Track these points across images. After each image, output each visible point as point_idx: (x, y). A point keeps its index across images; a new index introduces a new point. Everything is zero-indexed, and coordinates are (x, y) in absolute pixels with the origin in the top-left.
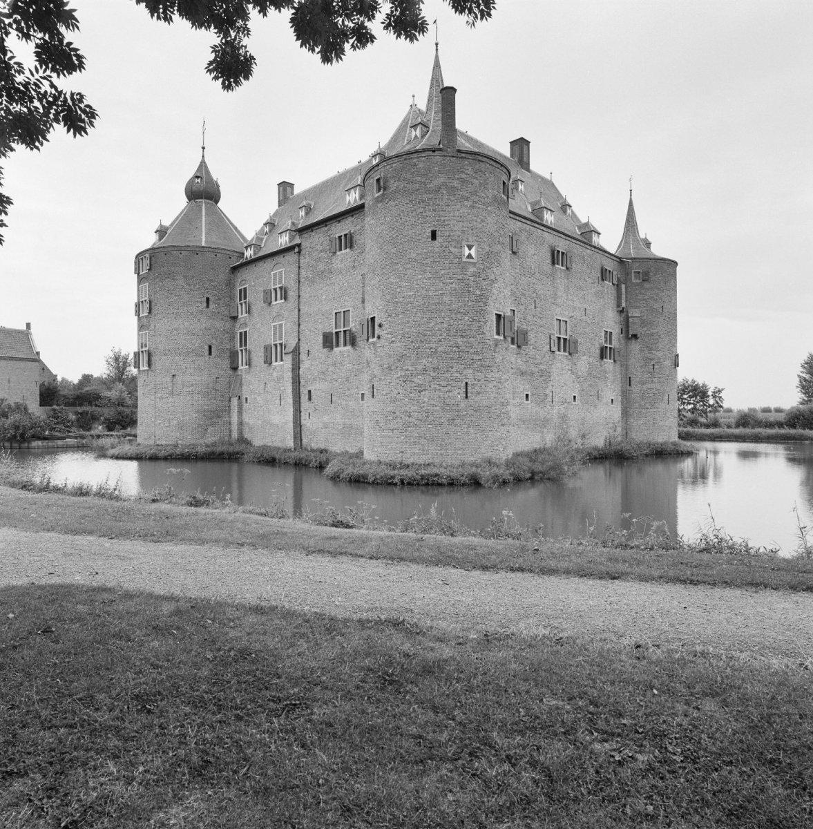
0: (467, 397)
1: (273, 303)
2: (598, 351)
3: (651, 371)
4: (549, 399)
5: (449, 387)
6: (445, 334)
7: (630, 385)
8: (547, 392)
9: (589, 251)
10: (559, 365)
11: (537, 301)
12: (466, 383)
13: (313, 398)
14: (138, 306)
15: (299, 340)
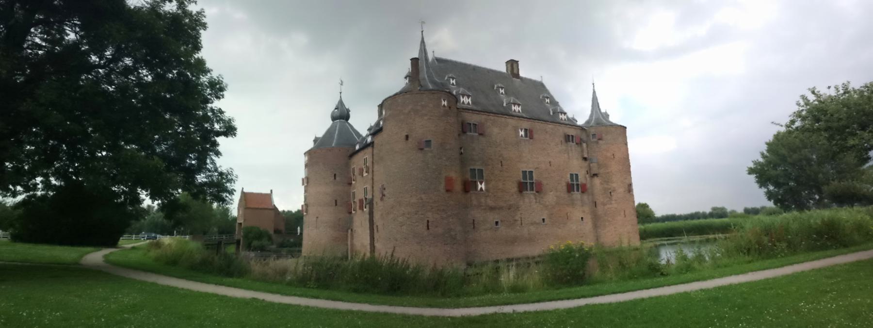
0: (428, 229)
1: (364, 175)
2: (565, 188)
3: (610, 196)
4: (519, 222)
5: (417, 224)
6: (414, 193)
7: (596, 206)
8: (517, 218)
9: (550, 126)
10: (527, 200)
11: (504, 162)
12: (428, 221)
13: (379, 230)
14: (303, 180)
15: (373, 196)
